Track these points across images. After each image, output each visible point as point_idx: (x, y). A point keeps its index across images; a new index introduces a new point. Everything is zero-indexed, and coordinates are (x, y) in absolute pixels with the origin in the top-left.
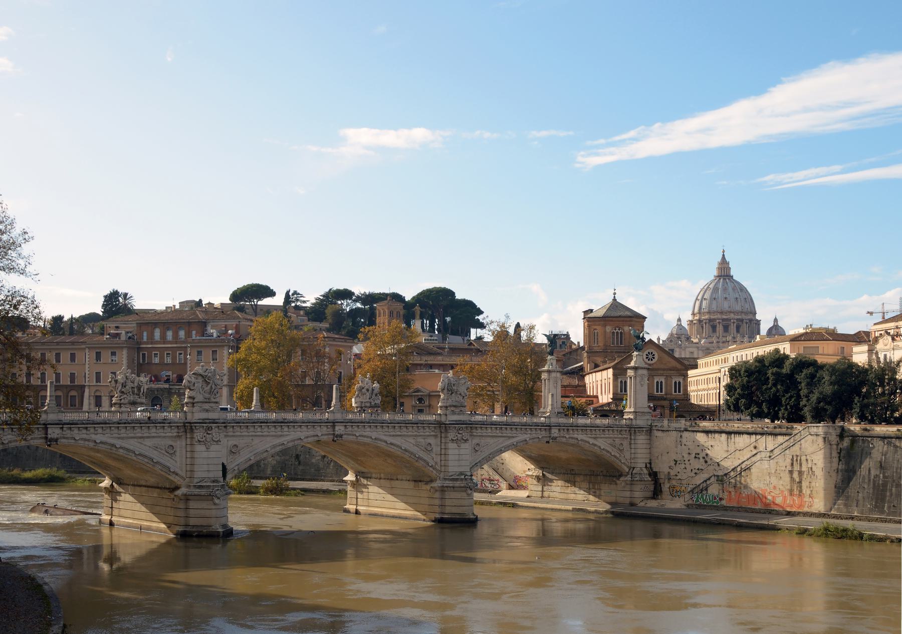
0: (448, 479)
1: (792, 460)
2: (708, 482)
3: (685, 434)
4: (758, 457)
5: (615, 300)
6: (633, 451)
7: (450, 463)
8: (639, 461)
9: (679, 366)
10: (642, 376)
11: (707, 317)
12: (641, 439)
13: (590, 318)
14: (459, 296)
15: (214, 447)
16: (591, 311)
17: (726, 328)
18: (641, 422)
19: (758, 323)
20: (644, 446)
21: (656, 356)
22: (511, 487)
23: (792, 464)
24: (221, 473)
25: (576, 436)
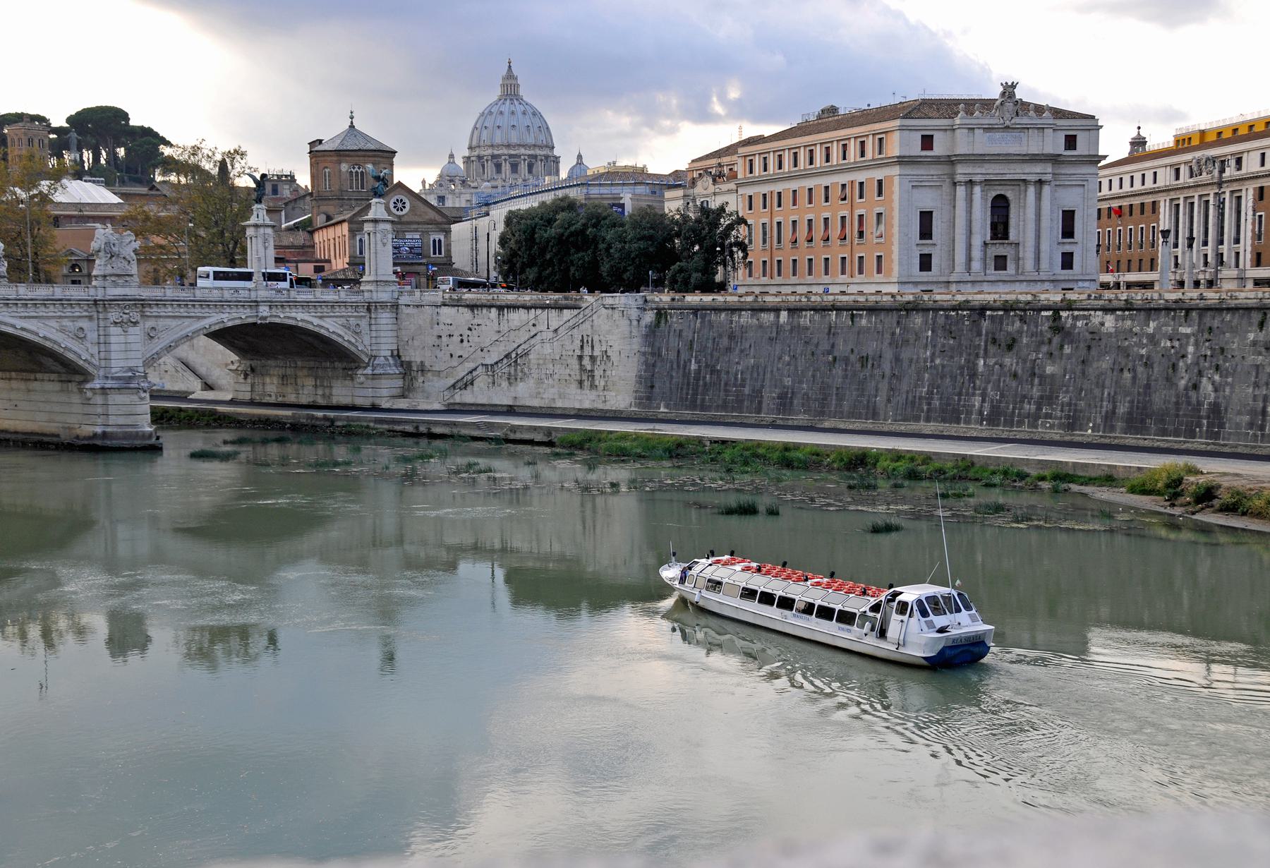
0: (113, 378)
1: (582, 341)
2: (475, 374)
3: (445, 310)
4: (538, 337)
5: (352, 126)
6: (374, 334)
7: (113, 356)
8: (383, 347)
9: (439, 218)
10: (384, 232)
11: (489, 151)
12: (385, 317)
13: (317, 153)
14: (134, 122)
16: (320, 141)
17: (515, 168)
18: (384, 295)
19: (556, 160)
20: (390, 327)
21: (408, 205)
22: (208, 387)
23: (582, 347)
25: (293, 315)
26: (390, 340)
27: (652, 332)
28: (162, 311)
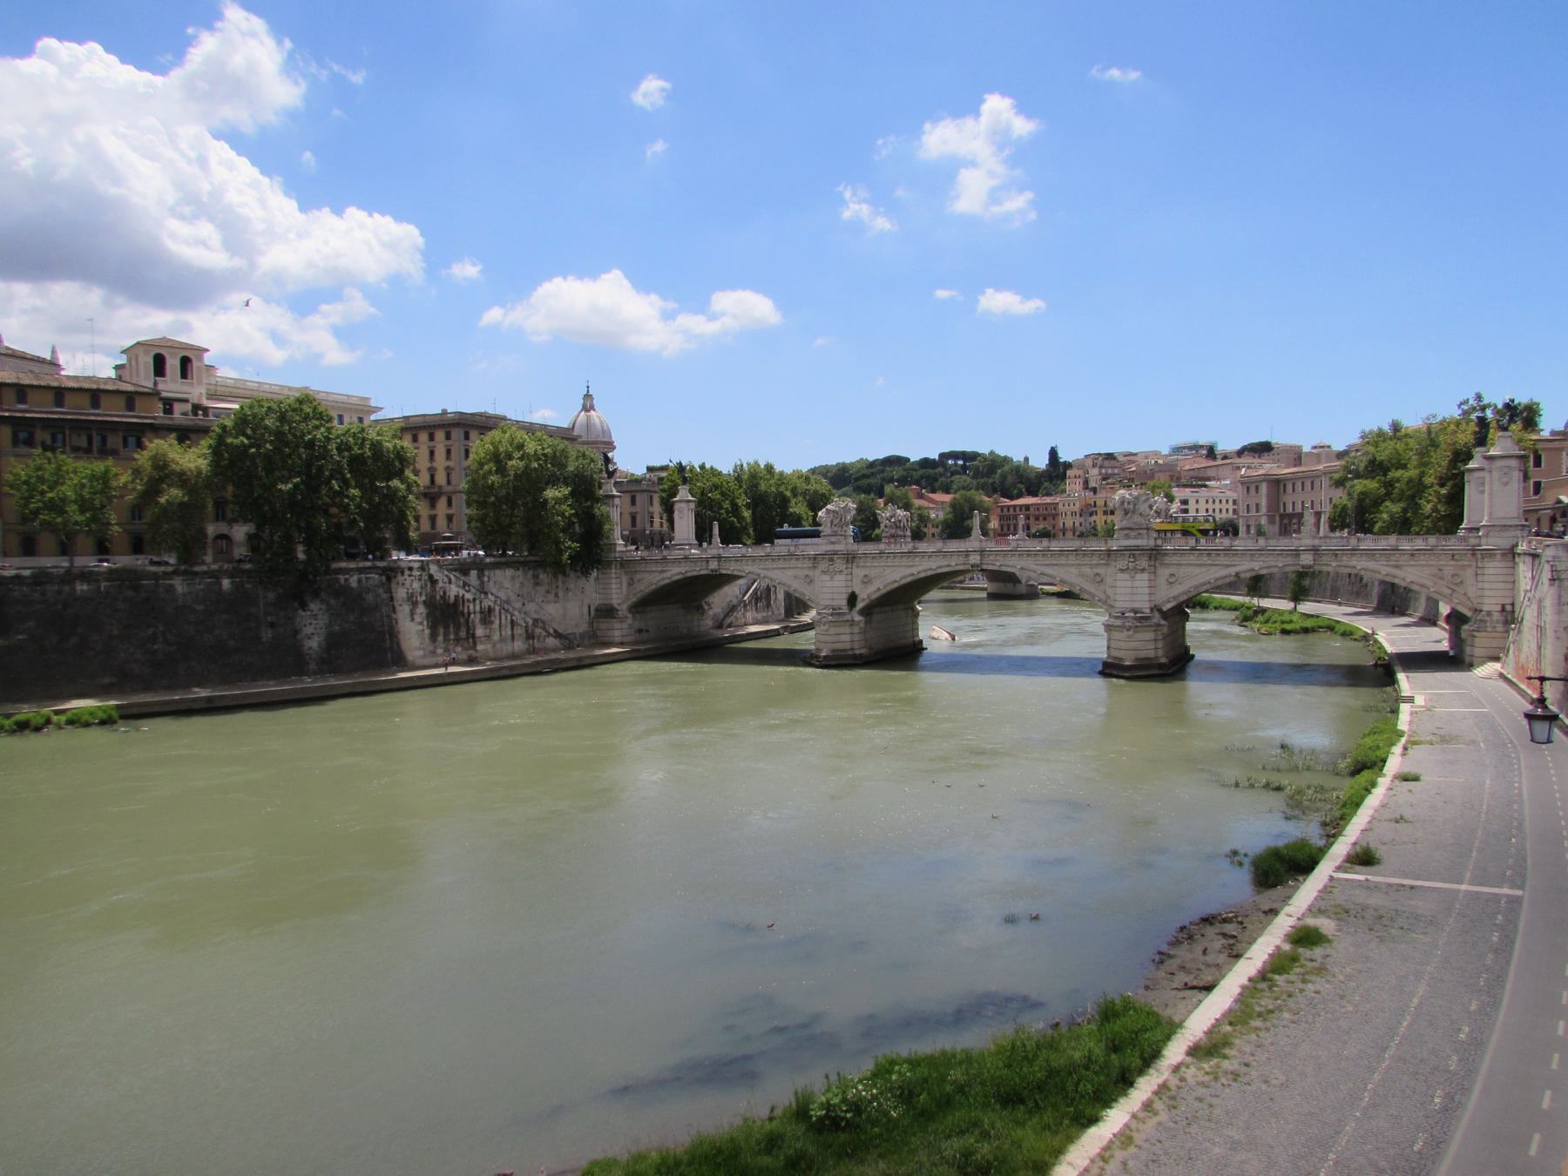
6: (1480, 585)
8: (1486, 600)
12: (1493, 568)
15: (838, 577)
20: (1501, 578)
24: (844, 602)
25: (1354, 563)
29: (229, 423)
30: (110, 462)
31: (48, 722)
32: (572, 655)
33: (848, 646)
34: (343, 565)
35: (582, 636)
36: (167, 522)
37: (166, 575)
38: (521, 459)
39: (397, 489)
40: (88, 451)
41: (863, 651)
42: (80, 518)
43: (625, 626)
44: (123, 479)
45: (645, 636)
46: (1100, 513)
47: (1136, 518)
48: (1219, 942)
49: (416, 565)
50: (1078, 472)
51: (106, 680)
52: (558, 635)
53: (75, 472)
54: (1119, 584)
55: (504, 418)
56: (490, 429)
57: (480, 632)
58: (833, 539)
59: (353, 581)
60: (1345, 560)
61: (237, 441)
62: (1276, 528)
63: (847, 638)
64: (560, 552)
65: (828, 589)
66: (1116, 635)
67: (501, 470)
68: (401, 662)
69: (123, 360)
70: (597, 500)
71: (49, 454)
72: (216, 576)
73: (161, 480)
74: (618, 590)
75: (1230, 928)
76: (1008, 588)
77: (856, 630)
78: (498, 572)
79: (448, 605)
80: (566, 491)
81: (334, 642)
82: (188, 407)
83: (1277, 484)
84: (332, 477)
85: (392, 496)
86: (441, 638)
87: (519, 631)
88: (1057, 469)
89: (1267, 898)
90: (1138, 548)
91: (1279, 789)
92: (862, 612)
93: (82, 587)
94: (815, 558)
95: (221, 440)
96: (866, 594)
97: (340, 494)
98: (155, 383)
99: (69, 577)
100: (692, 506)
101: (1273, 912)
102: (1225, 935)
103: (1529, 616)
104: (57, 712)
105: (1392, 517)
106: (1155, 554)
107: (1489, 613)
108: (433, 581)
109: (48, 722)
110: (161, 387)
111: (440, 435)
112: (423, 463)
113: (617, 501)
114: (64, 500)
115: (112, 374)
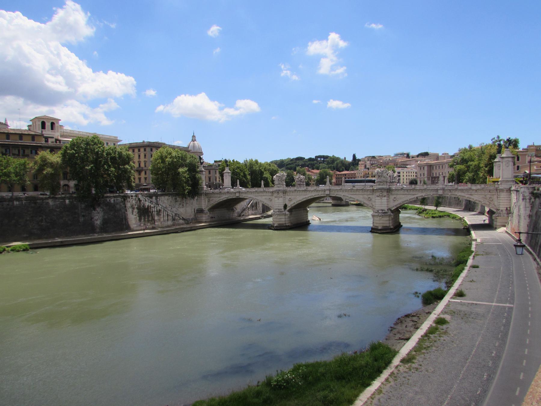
8: (501, 206)
12: (503, 195)
20: (506, 199)
24: (283, 207)
26: (505, 204)
27: (532, 205)
28: (399, 192)
29: (68, 145)
30: (26, 159)
31: (4, 250)
32: (188, 226)
33: (284, 223)
34: (108, 195)
35: (192, 219)
36: (47, 180)
37: (46, 199)
38: (170, 158)
39: (128, 169)
40: (18, 155)
41: (289, 224)
42: (16, 179)
43: (207, 216)
44: (31, 165)
45: (214, 219)
46: (370, 176)
47: (383, 178)
48: (411, 323)
49: (134, 195)
50: (363, 163)
51: (25, 235)
52: (183, 219)
53: (14, 163)
54: (377, 201)
55: (164, 144)
56: (159, 147)
57: (156, 218)
58: (279, 186)
59: (112, 201)
60: (453, 193)
61: (71, 152)
62: (430, 182)
63: (283, 220)
64: (184, 190)
65: (277, 203)
66: (376, 218)
67: (163, 161)
68: (129, 228)
69: (31, 123)
70: (197, 172)
71: (4, 156)
72: (64, 199)
73: (44, 165)
74: (204, 204)
75: (415, 319)
76: (339, 202)
77: (287, 217)
78: (162, 197)
79: (145, 209)
80: (186, 169)
81: (105, 222)
82: (54, 140)
83: (430, 166)
84: (104, 164)
85: (126, 171)
86: (143, 220)
87: (170, 218)
88: (355, 162)
89: (427, 309)
90: (383, 189)
91: (431, 271)
92: (289, 211)
93: (16, 203)
94: (272, 192)
95: (65, 151)
96: (290, 205)
97: (108, 170)
98: (42, 132)
99: (12, 199)
100: (230, 174)
101: (429, 313)
102: (413, 321)
103: (515, 211)
104: (8, 247)
105: (469, 178)
106: (389, 190)
107: (502, 211)
108: (140, 201)
109: (4, 250)
110: (44, 133)
111: (142, 150)
112: (136, 159)
113: (204, 173)
114: (10, 172)
115: (27, 128)
